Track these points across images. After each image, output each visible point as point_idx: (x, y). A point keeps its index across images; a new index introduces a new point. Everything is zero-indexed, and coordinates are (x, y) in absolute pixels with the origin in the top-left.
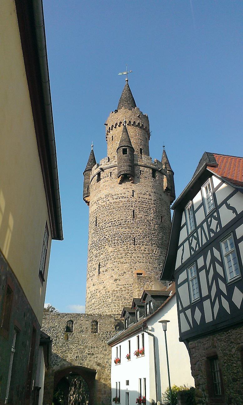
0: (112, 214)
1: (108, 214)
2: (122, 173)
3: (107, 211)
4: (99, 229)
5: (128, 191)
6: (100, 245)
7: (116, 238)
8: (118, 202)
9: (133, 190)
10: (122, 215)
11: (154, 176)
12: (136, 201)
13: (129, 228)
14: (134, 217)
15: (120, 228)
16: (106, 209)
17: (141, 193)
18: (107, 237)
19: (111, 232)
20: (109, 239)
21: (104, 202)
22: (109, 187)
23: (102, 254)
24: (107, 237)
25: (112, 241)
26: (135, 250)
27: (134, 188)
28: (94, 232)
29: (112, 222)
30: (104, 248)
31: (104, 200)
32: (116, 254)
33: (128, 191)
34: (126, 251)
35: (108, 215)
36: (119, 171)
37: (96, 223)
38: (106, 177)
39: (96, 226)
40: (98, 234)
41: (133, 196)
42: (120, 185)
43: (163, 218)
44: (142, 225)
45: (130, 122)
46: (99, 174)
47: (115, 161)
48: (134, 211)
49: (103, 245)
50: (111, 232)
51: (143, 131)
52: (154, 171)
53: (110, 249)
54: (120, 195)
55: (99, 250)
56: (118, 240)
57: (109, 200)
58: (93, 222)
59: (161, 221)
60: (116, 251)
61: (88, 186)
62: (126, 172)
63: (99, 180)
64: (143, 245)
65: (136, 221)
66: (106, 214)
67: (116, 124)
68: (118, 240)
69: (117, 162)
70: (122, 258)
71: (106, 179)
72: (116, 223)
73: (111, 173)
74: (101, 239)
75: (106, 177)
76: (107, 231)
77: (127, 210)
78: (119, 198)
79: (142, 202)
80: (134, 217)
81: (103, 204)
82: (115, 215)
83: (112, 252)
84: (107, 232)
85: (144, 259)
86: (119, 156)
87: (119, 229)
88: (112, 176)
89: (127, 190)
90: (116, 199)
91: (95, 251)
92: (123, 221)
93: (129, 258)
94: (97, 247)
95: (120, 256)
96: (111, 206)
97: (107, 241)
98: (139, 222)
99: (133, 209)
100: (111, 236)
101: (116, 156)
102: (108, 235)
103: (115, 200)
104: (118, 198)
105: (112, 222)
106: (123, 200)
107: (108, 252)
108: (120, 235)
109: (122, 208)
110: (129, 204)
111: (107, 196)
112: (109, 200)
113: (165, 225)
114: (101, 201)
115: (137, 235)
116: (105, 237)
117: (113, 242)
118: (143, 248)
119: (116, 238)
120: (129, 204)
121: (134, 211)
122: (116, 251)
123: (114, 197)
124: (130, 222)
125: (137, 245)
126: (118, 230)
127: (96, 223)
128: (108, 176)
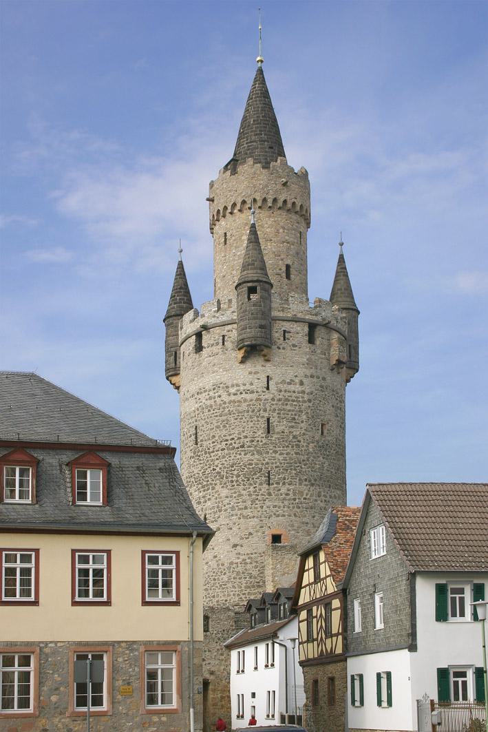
0: (228, 426)
1: (219, 424)
2: (246, 343)
3: (217, 418)
4: (203, 452)
5: (259, 379)
6: (205, 483)
7: (236, 472)
8: (239, 401)
9: (268, 377)
10: (246, 429)
11: (311, 340)
12: (273, 399)
13: (259, 453)
14: (269, 432)
15: (243, 453)
16: (216, 414)
17: (283, 382)
18: (218, 469)
19: (226, 461)
20: (222, 473)
21: (210, 398)
22: (220, 368)
23: (209, 499)
24: (218, 469)
25: (227, 478)
26: (270, 494)
27: (270, 373)
28: (192, 455)
29: (227, 440)
30: (213, 488)
31: (211, 393)
32: (235, 500)
33: (259, 379)
34: (254, 497)
35: (218, 427)
36: (241, 337)
37: (196, 438)
38: (212, 345)
39: (197, 444)
40: (201, 462)
41: (268, 388)
42: (242, 366)
43: (327, 427)
44: (283, 447)
45: (265, 200)
46: (199, 336)
47: (233, 312)
48: (268, 419)
49: (211, 484)
50: (226, 461)
51: (294, 217)
52: (312, 327)
53: (224, 492)
54: (242, 388)
55: (204, 491)
56: (238, 476)
57: (220, 396)
58: (189, 434)
59: (322, 433)
60: (234, 495)
61: (176, 353)
62: (255, 340)
63: (199, 348)
64: (284, 484)
65: (273, 439)
66: (216, 425)
67: (234, 205)
68: (238, 476)
69: (236, 314)
70: (246, 508)
71: (215, 349)
72: (235, 443)
73: (224, 336)
74: (207, 473)
75: (212, 345)
76: (217, 457)
77: (255, 419)
78: (241, 393)
79: (287, 400)
80: (269, 432)
81: (208, 403)
82: (233, 427)
83: (227, 497)
84: (217, 459)
85: (285, 509)
86: (240, 303)
87: (240, 454)
88: (225, 343)
89: (256, 376)
90: (234, 394)
91: (197, 493)
92: (248, 440)
93: (259, 509)
94: (200, 486)
95: (241, 505)
96: (224, 408)
97: (217, 477)
98: (277, 441)
99: (266, 415)
100: (225, 468)
101: (234, 301)
102: (220, 466)
103: (233, 398)
104: (239, 393)
105: (227, 440)
106: (248, 397)
107: (221, 498)
108: (243, 467)
109: (246, 414)
110: (260, 405)
111: (216, 387)
112: (220, 396)
113: (330, 438)
114: (204, 394)
115: (274, 466)
116: (214, 469)
117: (230, 479)
118: (283, 490)
119: (236, 472)
120: (260, 405)
121: (268, 419)
122: (234, 495)
123: (233, 390)
124: (262, 441)
125: (273, 484)
126: (238, 457)
127: (196, 438)
128: (217, 344)
